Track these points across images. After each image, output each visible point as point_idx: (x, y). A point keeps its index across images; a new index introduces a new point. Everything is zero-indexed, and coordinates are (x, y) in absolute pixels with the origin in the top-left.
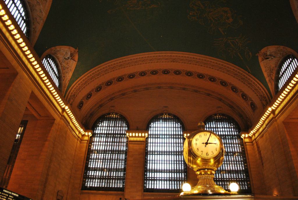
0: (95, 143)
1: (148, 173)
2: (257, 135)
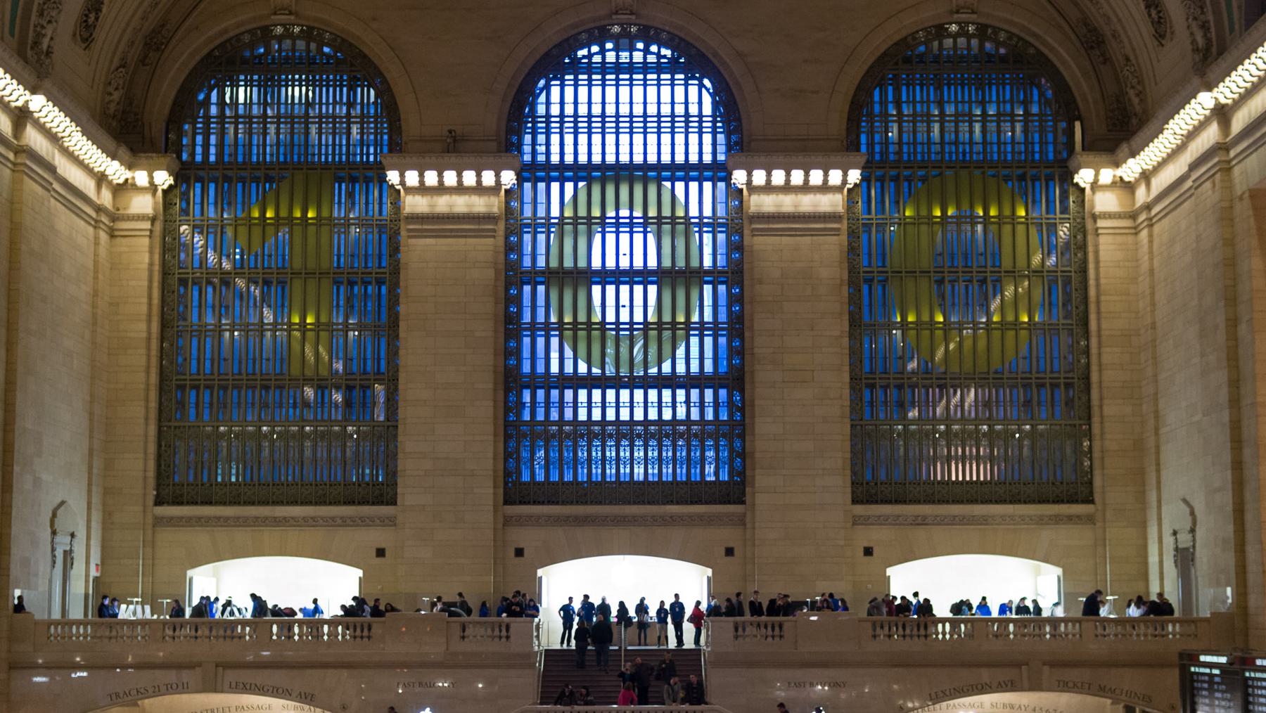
1: (527, 396)
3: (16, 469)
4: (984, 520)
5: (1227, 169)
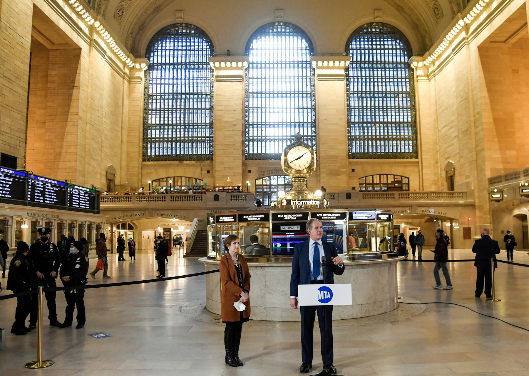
0: (155, 82)
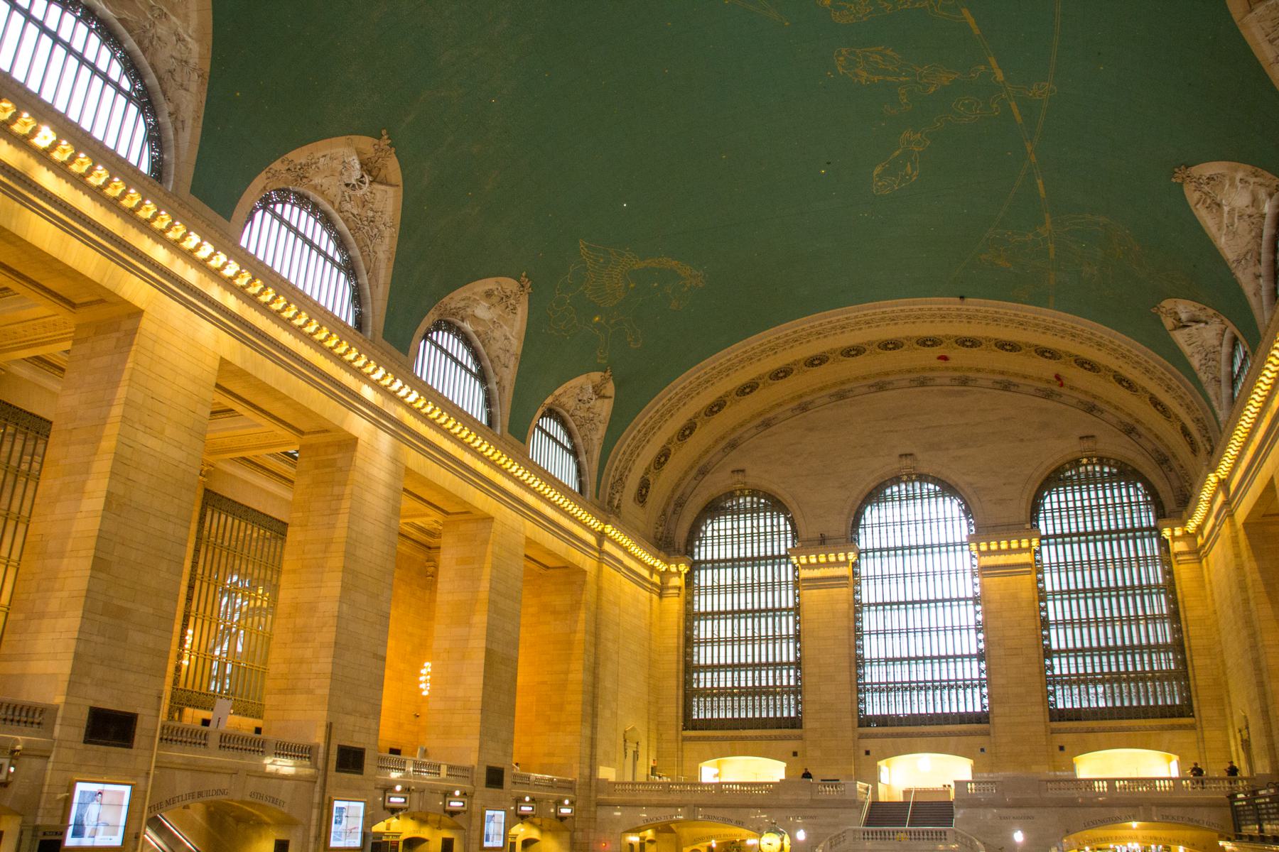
1: (868, 669)
2: (1206, 532)
3: (600, 706)
4: (1129, 729)
5: (1231, 515)
